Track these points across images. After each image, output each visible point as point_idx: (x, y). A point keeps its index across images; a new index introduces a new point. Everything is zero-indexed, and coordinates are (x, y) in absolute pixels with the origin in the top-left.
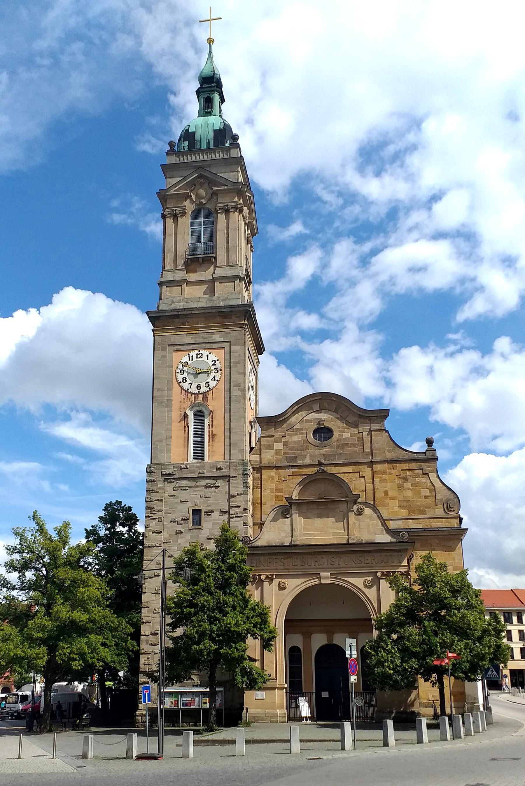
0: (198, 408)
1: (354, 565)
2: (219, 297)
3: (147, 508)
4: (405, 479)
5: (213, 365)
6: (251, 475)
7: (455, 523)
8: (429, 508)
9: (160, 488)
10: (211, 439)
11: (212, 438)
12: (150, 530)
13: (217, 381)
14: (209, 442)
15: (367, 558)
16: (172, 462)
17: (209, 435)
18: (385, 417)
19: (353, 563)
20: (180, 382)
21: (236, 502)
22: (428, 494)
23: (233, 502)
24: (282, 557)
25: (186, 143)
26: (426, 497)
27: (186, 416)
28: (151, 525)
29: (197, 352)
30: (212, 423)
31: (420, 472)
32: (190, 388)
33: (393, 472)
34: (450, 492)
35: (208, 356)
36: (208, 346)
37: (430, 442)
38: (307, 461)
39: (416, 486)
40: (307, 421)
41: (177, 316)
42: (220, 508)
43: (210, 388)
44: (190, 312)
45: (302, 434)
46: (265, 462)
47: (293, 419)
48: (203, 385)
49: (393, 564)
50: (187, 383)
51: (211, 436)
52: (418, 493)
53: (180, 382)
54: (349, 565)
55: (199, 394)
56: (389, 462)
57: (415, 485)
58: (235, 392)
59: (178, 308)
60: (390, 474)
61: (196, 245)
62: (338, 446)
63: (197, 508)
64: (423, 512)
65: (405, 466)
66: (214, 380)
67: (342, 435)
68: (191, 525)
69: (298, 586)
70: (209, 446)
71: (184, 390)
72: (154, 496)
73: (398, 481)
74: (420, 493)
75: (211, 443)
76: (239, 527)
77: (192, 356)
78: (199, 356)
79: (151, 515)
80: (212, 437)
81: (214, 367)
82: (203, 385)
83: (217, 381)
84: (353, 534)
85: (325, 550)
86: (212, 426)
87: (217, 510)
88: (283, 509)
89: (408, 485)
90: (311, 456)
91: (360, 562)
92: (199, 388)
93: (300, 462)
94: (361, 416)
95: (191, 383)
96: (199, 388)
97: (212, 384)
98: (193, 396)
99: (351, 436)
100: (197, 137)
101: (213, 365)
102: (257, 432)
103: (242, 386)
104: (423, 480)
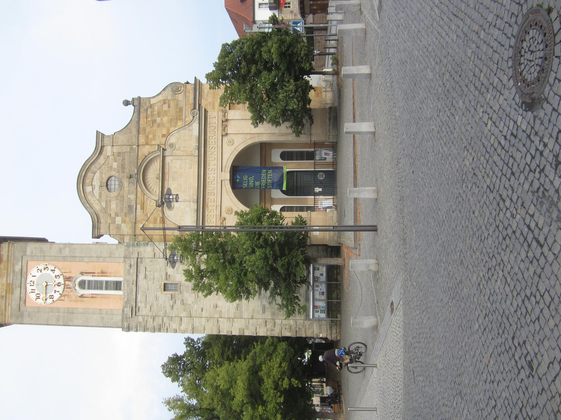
1: (216, 153)
3: (160, 330)
4: (154, 121)
5: (41, 271)
7: (190, 88)
8: (177, 105)
9: (143, 320)
11: (104, 273)
12: (179, 328)
14: (107, 276)
15: (210, 142)
16: (122, 308)
17: (102, 276)
18: (103, 135)
22: (167, 105)
23: (159, 256)
24: (206, 211)
26: (169, 107)
27: (82, 296)
28: (174, 327)
29: (28, 286)
30: (91, 273)
33: (148, 130)
36: (24, 276)
37: (126, 103)
38: (132, 197)
40: (100, 196)
42: (164, 267)
45: (110, 201)
46: (130, 232)
47: (97, 207)
48: (58, 281)
50: (54, 294)
55: (65, 284)
56: (139, 133)
57: (159, 115)
58: (66, 252)
60: (149, 132)
62: (123, 172)
64: (181, 110)
67: (115, 169)
68: (177, 293)
70: (110, 276)
71: (60, 297)
72: (150, 324)
73: (155, 127)
74: (166, 111)
75: (108, 275)
78: (32, 284)
79: (166, 328)
80: (103, 273)
81: (43, 270)
82: (58, 281)
86: (94, 273)
87: (166, 269)
89: (158, 120)
90: (129, 194)
93: (133, 203)
94: (100, 153)
97: (57, 272)
98: (65, 290)
101: (41, 271)
102: (106, 239)
103: (62, 246)
104: (156, 108)
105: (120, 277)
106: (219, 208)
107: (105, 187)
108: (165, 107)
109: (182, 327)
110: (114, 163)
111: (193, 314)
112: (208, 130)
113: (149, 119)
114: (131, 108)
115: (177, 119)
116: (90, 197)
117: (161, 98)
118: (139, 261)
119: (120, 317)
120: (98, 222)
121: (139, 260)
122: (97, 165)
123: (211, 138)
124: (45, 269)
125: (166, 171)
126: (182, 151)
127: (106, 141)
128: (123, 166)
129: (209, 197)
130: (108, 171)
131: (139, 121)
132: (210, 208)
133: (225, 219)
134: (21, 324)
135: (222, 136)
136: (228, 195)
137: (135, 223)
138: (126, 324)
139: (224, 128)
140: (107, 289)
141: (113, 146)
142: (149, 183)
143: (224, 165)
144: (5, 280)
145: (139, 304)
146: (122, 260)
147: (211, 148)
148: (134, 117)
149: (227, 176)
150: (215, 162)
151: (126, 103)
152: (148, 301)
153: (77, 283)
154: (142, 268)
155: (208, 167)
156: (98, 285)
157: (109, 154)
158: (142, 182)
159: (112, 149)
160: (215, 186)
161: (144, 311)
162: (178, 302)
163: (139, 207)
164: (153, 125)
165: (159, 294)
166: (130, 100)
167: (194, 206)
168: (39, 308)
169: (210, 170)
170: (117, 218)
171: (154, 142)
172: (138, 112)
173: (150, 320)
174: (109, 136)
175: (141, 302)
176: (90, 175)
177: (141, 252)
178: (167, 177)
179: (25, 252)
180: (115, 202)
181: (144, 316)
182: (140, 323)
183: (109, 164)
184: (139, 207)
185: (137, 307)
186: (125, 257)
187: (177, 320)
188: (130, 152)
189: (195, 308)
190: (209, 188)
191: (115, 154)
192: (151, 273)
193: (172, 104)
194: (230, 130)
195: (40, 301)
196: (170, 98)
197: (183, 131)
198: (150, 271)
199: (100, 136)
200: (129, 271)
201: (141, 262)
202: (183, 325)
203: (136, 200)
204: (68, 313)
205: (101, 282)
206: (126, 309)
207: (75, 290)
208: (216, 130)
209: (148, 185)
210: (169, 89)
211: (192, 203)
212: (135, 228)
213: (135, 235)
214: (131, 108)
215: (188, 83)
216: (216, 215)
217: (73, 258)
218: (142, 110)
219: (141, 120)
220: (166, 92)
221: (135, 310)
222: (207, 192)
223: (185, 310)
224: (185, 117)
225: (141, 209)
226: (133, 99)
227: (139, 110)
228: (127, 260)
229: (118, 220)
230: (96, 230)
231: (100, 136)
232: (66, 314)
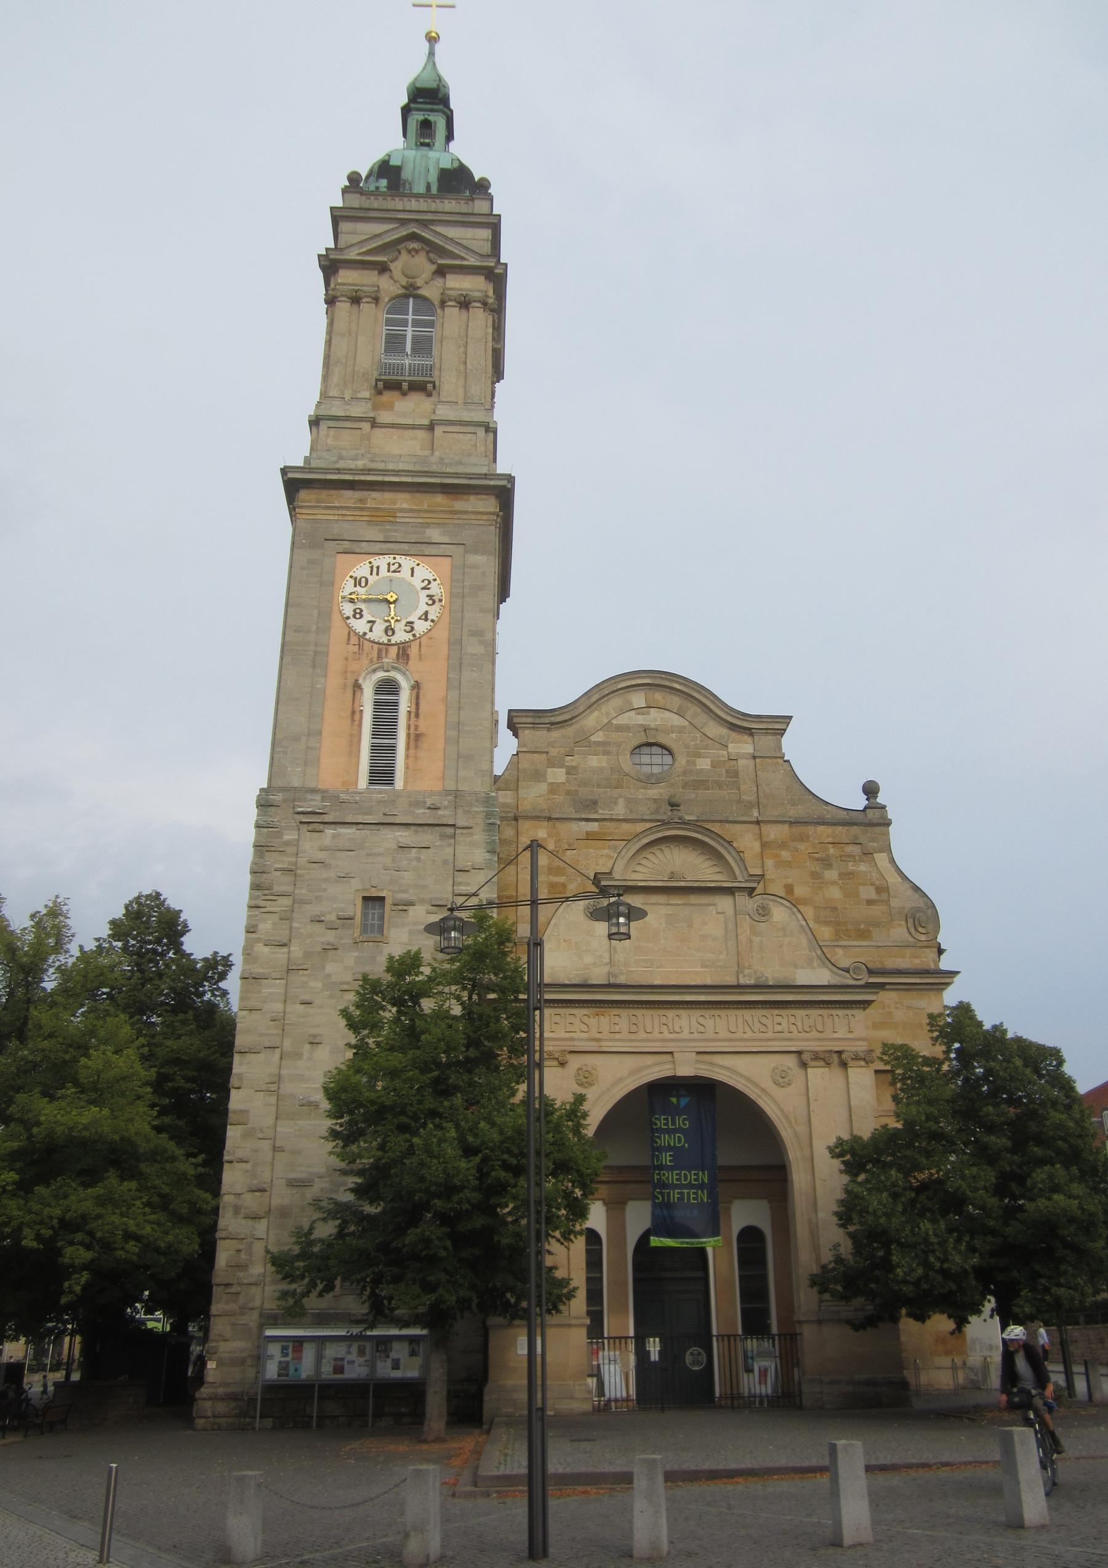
0: (386, 674)
1: (749, 1034)
2: (442, 459)
3: (255, 887)
4: (826, 863)
5: (423, 588)
7: (926, 959)
8: (877, 925)
9: (287, 844)
10: (412, 742)
12: (258, 940)
13: (433, 621)
14: (408, 748)
15: (779, 1019)
16: (320, 786)
17: (408, 735)
19: (747, 1029)
20: (348, 618)
22: (873, 895)
23: (460, 884)
24: (585, 1011)
25: (383, 183)
26: (870, 902)
27: (357, 687)
29: (389, 559)
30: (417, 708)
31: (855, 850)
32: (371, 630)
33: (802, 846)
34: (917, 896)
35: (412, 569)
36: (414, 549)
37: (871, 790)
38: (620, 810)
40: (619, 728)
41: (351, 485)
43: (414, 635)
44: (380, 478)
45: (607, 753)
46: (526, 806)
48: (400, 628)
49: (836, 1036)
50: (364, 620)
51: (412, 736)
53: (348, 618)
54: (739, 1035)
57: (846, 875)
58: (473, 648)
59: (352, 466)
61: (394, 360)
62: (685, 785)
63: (374, 893)
64: (864, 934)
66: (426, 619)
67: (694, 763)
69: (621, 1080)
70: (407, 757)
71: (356, 634)
72: (274, 861)
75: (412, 752)
77: (378, 568)
78: (393, 568)
79: (262, 903)
80: (416, 738)
81: (427, 592)
82: (400, 628)
83: (433, 621)
84: (746, 964)
86: (417, 716)
87: (422, 901)
89: (832, 875)
90: (628, 800)
91: (763, 1029)
92: (390, 633)
94: (733, 727)
95: (373, 622)
96: (390, 633)
97: (421, 627)
98: (376, 647)
99: (713, 766)
100: (406, 174)
101: (423, 588)
102: (507, 745)
103: (488, 637)
104: (863, 867)
105: (406, 782)
106: (592, 1046)
107: (644, 740)
109: (261, 949)
110: (708, 761)
111: (296, 978)
112: (814, 1013)
113: (832, 851)
114: (859, 802)
116: (616, 702)
117: (893, 879)
118: (448, 829)
119: (296, 783)
120: (552, 724)
121: (450, 830)
122: (702, 718)
123: (792, 1020)
124: (430, 597)
125: (694, 899)
126: (751, 942)
127: (769, 740)
128: (701, 783)
129: (623, 1019)
130: (687, 747)
131: (824, 824)
132: (593, 1021)
133: (562, 1064)
134: (293, 543)
135: (799, 1053)
136: (631, 1074)
137: (550, 819)
138: (278, 798)
139: (823, 1058)
140: (374, 748)
141: (755, 758)
142: (658, 853)
143: (717, 1059)
144: (405, 506)
145: (329, 831)
146: (451, 785)
147: (764, 1020)
148: (834, 810)
149: (686, 1069)
150: (723, 1034)
151: (871, 790)
152: (339, 854)
153: (392, 674)
154: (427, 837)
155: (708, 1013)
156: (385, 725)
157: (733, 748)
158: (660, 835)
159: (744, 756)
161: (311, 845)
162: (330, 937)
163: (594, 827)
164: (818, 859)
165: (356, 884)
166: (881, 799)
167: (598, 976)
168: (332, 584)
169: (702, 1021)
170: (563, 770)
171: (769, 863)
172: (848, 819)
173: (285, 862)
174: (780, 747)
175: (334, 836)
176: (676, 701)
177: (471, 834)
178: (676, 900)
179: (476, 551)
180: (604, 764)
181: (297, 846)
182: (279, 835)
183: (707, 747)
184: (594, 827)
185: (321, 827)
186: (457, 794)
187: (282, 935)
188: (739, 801)
189: (312, 984)
190: (648, 1019)
191: (732, 763)
192: (414, 863)
193: (877, 911)
194: (817, 1075)
195: (348, 587)
196: (895, 903)
197: (804, 942)
198: (419, 859)
199: (777, 725)
200: (418, 804)
201: (443, 836)
202: (266, 949)
203: (611, 820)
204: (316, 653)
205: (393, 734)
206: (318, 797)
207: (374, 671)
208: (814, 1034)
209: (654, 849)
210: (921, 903)
211: (606, 969)
212: (537, 818)
213: (516, 819)
214: (859, 802)
215: (940, 951)
216: (573, 1039)
217: (457, 662)
218: (855, 830)
219: (829, 830)
220: (910, 892)
221: (314, 822)
222: (639, 1013)
223: (308, 955)
225: (587, 833)
226: (884, 807)
228: (451, 798)
229: (558, 775)
230: (529, 720)
231: (777, 725)
232: (313, 648)
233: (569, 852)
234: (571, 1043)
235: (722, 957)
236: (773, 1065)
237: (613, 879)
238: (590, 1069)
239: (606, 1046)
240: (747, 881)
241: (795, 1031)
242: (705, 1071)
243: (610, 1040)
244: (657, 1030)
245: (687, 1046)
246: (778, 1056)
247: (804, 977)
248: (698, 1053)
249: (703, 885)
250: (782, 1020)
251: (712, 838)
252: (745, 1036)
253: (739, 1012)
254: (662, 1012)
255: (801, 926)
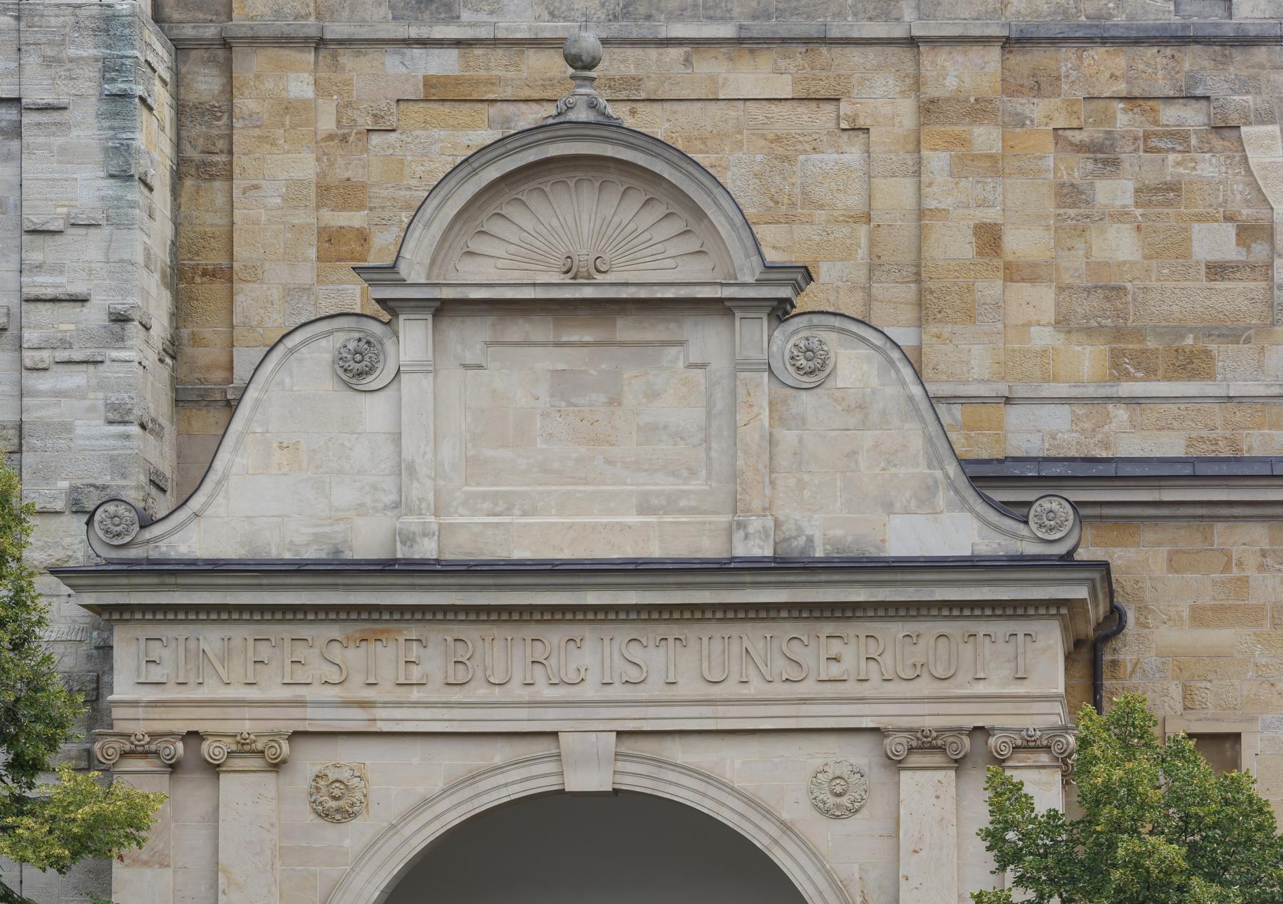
1: (756, 688)
4: (1104, 155)
6: (162, 98)
8: (1234, 334)
15: (836, 647)
19: (752, 672)
21: (59, 269)
24: (334, 631)
26: (1218, 270)
31: (1191, 117)
33: (1038, 110)
39: (1168, 203)
52: (1172, 249)
64: (1190, 364)
65: (1105, 66)
69: (426, 802)
73: (1057, 166)
74: (1179, 248)
76: (81, 427)
84: (756, 504)
85: (592, 598)
88: (340, 338)
89: (1115, 192)
91: (794, 674)
104: (1208, 167)
106: (353, 719)
108: (1215, 242)
113: (1123, 119)
115: (1119, 334)
125: (626, 329)
126: (772, 441)
131: (1104, 41)
132: (354, 656)
133: (277, 766)
137: (320, 43)
142: (496, 227)
143: (676, 751)
150: (690, 687)
160: (516, 691)
163: (444, 63)
164: (1080, 148)
167: (367, 541)
169: (635, 652)
171: (937, 161)
184: (444, 63)
193: (1236, 297)
197: (917, 443)
203: (495, 43)
212: (284, 41)
216: (302, 703)
218: (1192, 60)
219: (1117, 60)
222: (472, 633)
224: (1132, 401)
225: (429, 82)
227: (1196, 40)
233: (375, 139)
234: (297, 712)
235: (696, 485)
236: (818, 762)
237: (402, 283)
238: (345, 775)
239: (386, 719)
240: (760, 283)
241: (875, 677)
242: (637, 779)
243: (398, 704)
244: (518, 678)
245: (587, 719)
246: (831, 742)
247: (909, 536)
248: (619, 733)
249: (643, 293)
250: (848, 649)
251: (669, 162)
252: (746, 691)
253: (734, 630)
254: (530, 631)
255: (911, 398)
